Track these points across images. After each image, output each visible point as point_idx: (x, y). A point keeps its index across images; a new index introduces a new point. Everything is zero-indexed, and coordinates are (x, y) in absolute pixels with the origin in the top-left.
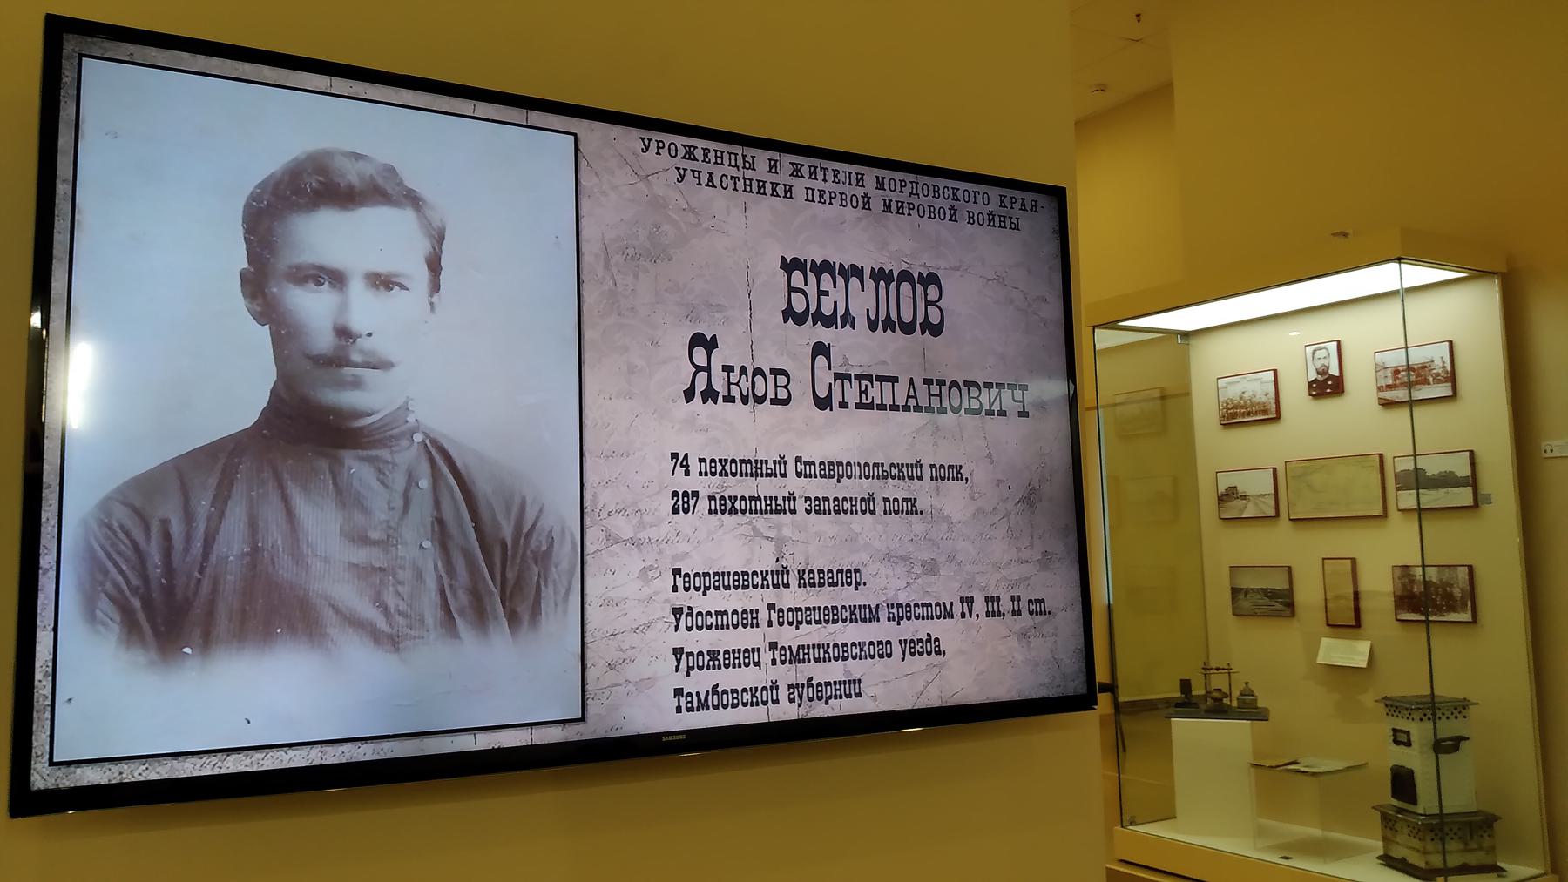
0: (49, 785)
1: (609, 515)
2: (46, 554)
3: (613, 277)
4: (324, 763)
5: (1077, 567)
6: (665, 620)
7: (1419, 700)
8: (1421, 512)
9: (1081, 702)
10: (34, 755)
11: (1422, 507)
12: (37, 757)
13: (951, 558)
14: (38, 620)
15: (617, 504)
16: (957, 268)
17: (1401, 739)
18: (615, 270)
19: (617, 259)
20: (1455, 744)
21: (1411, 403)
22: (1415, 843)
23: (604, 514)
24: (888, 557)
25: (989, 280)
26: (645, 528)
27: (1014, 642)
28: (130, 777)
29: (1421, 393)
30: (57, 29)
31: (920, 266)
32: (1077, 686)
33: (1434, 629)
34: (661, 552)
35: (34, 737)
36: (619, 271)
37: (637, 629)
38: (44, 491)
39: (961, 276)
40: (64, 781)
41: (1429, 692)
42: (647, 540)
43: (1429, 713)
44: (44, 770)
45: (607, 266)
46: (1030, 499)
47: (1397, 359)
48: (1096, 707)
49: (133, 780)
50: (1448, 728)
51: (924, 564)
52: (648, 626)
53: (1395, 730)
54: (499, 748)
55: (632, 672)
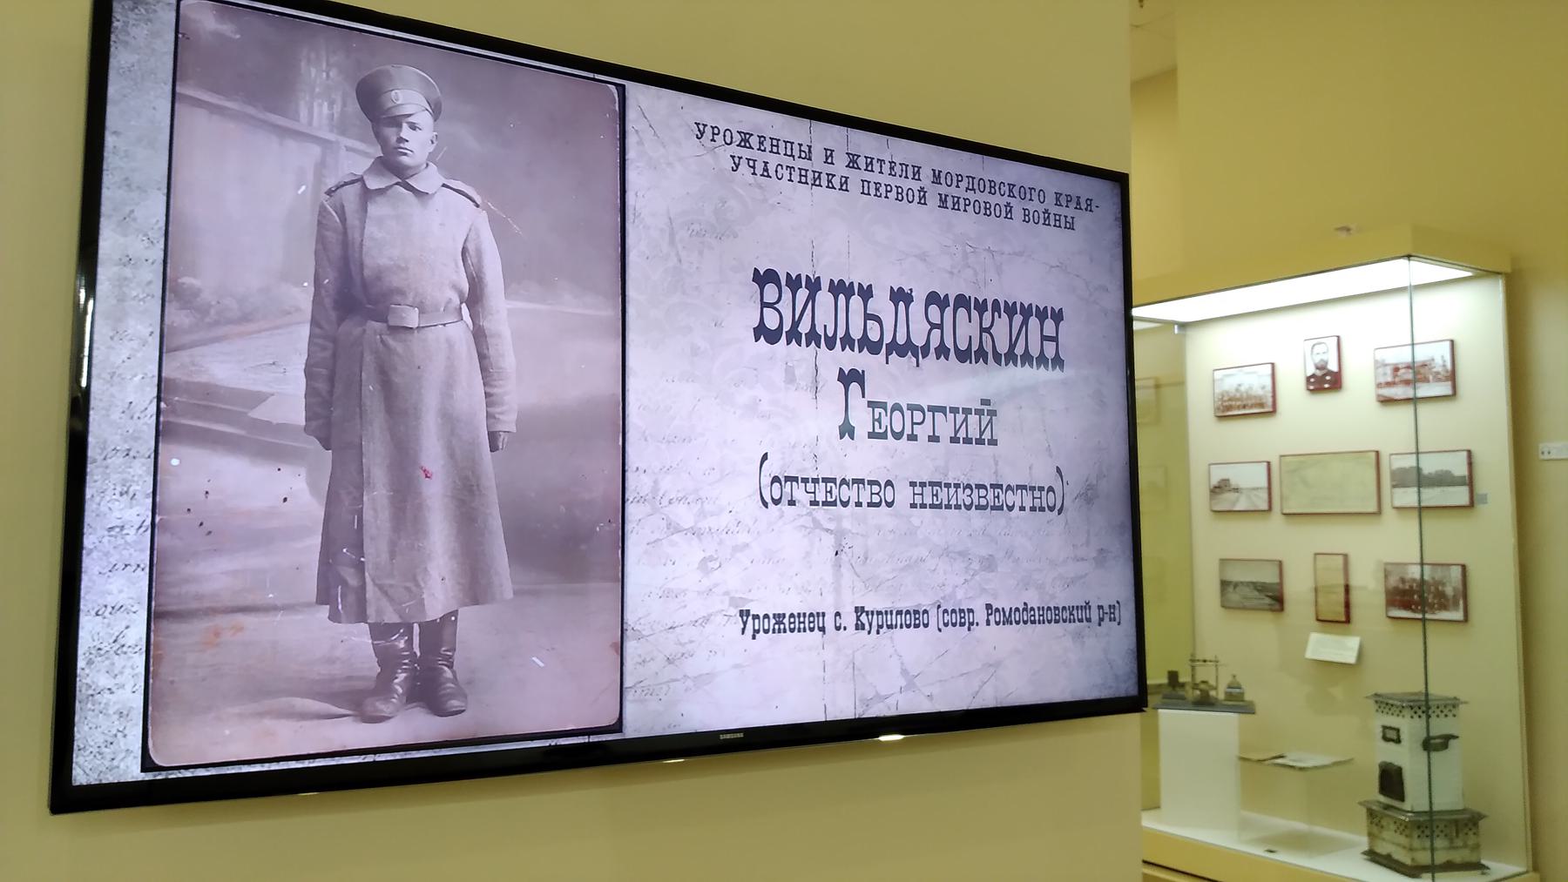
0: (91, 780)
1: (670, 503)
3: (677, 254)
5: (1131, 565)
6: (724, 613)
7: (1413, 698)
8: (1421, 509)
9: (1134, 703)
10: (75, 747)
11: (1423, 504)
12: (79, 750)
13: (1009, 554)
15: (678, 491)
16: (1020, 254)
17: (1392, 736)
18: (680, 247)
20: (1445, 741)
21: (1414, 401)
22: (1402, 840)
23: (665, 502)
24: (946, 552)
25: (1052, 267)
26: (705, 517)
29: (1424, 391)
31: (985, 250)
32: (1128, 688)
33: (1430, 627)
34: (721, 542)
35: (76, 729)
40: (108, 776)
41: (1422, 688)
42: (708, 530)
43: (1420, 712)
44: (86, 764)
45: (672, 242)
47: (1404, 356)
48: (1144, 709)
50: (1440, 726)
52: (707, 619)
53: (1385, 728)
55: (692, 667)
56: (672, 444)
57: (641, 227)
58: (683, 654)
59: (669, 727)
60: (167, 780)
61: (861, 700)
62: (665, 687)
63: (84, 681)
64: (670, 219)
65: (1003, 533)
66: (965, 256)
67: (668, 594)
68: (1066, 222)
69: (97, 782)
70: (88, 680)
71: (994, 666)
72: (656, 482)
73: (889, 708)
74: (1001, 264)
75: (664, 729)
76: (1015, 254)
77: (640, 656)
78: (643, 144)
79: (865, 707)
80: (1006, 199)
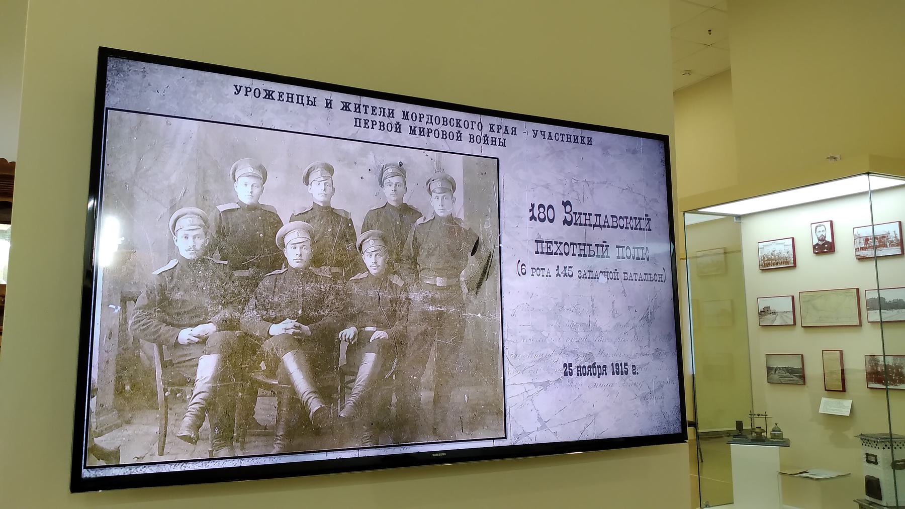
4: (242, 465)
7: (883, 437)
8: (882, 323)
9: (679, 438)
16: (604, 183)
17: (871, 460)
21: (876, 258)
25: (624, 189)
27: (638, 402)
28: (135, 471)
30: (105, 54)
32: (676, 429)
33: (890, 393)
43: (889, 445)
46: (648, 318)
47: (867, 232)
49: (137, 473)
51: (585, 355)
53: (867, 455)
54: (340, 459)
60: (130, 476)
61: (513, 435)
65: (597, 340)
66: (572, 185)
69: (94, 476)
74: (593, 189)
76: (601, 183)
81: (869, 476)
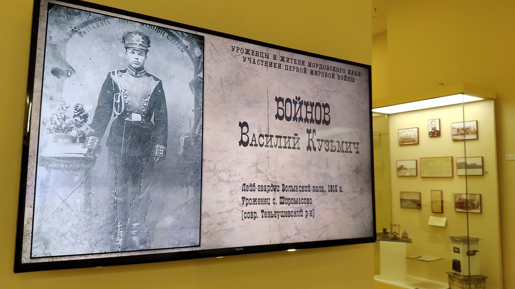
2: (29, 180)
3: (223, 91)
6: (237, 208)
8: (466, 176)
9: (372, 239)
10: (23, 251)
12: (24, 252)
14: (26, 203)
15: (223, 168)
16: (335, 91)
17: (457, 251)
18: (224, 88)
19: (225, 84)
20: (474, 252)
21: (464, 140)
22: (460, 285)
23: (218, 171)
25: (346, 96)
27: (351, 219)
29: (468, 137)
31: (324, 90)
33: (469, 215)
34: (236, 185)
35: (23, 245)
36: (225, 88)
37: (228, 211)
38: (29, 158)
39: (337, 94)
41: (467, 235)
43: (466, 243)
44: (26, 256)
45: (222, 86)
46: (357, 171)
47: (461, 126)
48: (376, 241)
50: (472, 248)
52: (231, 210)
53: (454, 248)
55: (226, 226)
56: (221, 152)
57: (211, 81)
58: (224, 222)
59: (219, 246)
60: (53, 262)
61: (282, 238)
62: (217, 232)
63: (26, 229)
64: (221, 79)
66: (318, 92)
67: (219, 202)
68: (352, 79)
69: (29, 263)
70: (27, 229)
71: (326, 227)
72: (215, 165)
73: (291, 240)
74: (329, 95)
75: (217, 247)
77: (209, 222)
78: (212, 54)
79: (284, 240)
80: (332, 72)
81: (456, 260)
